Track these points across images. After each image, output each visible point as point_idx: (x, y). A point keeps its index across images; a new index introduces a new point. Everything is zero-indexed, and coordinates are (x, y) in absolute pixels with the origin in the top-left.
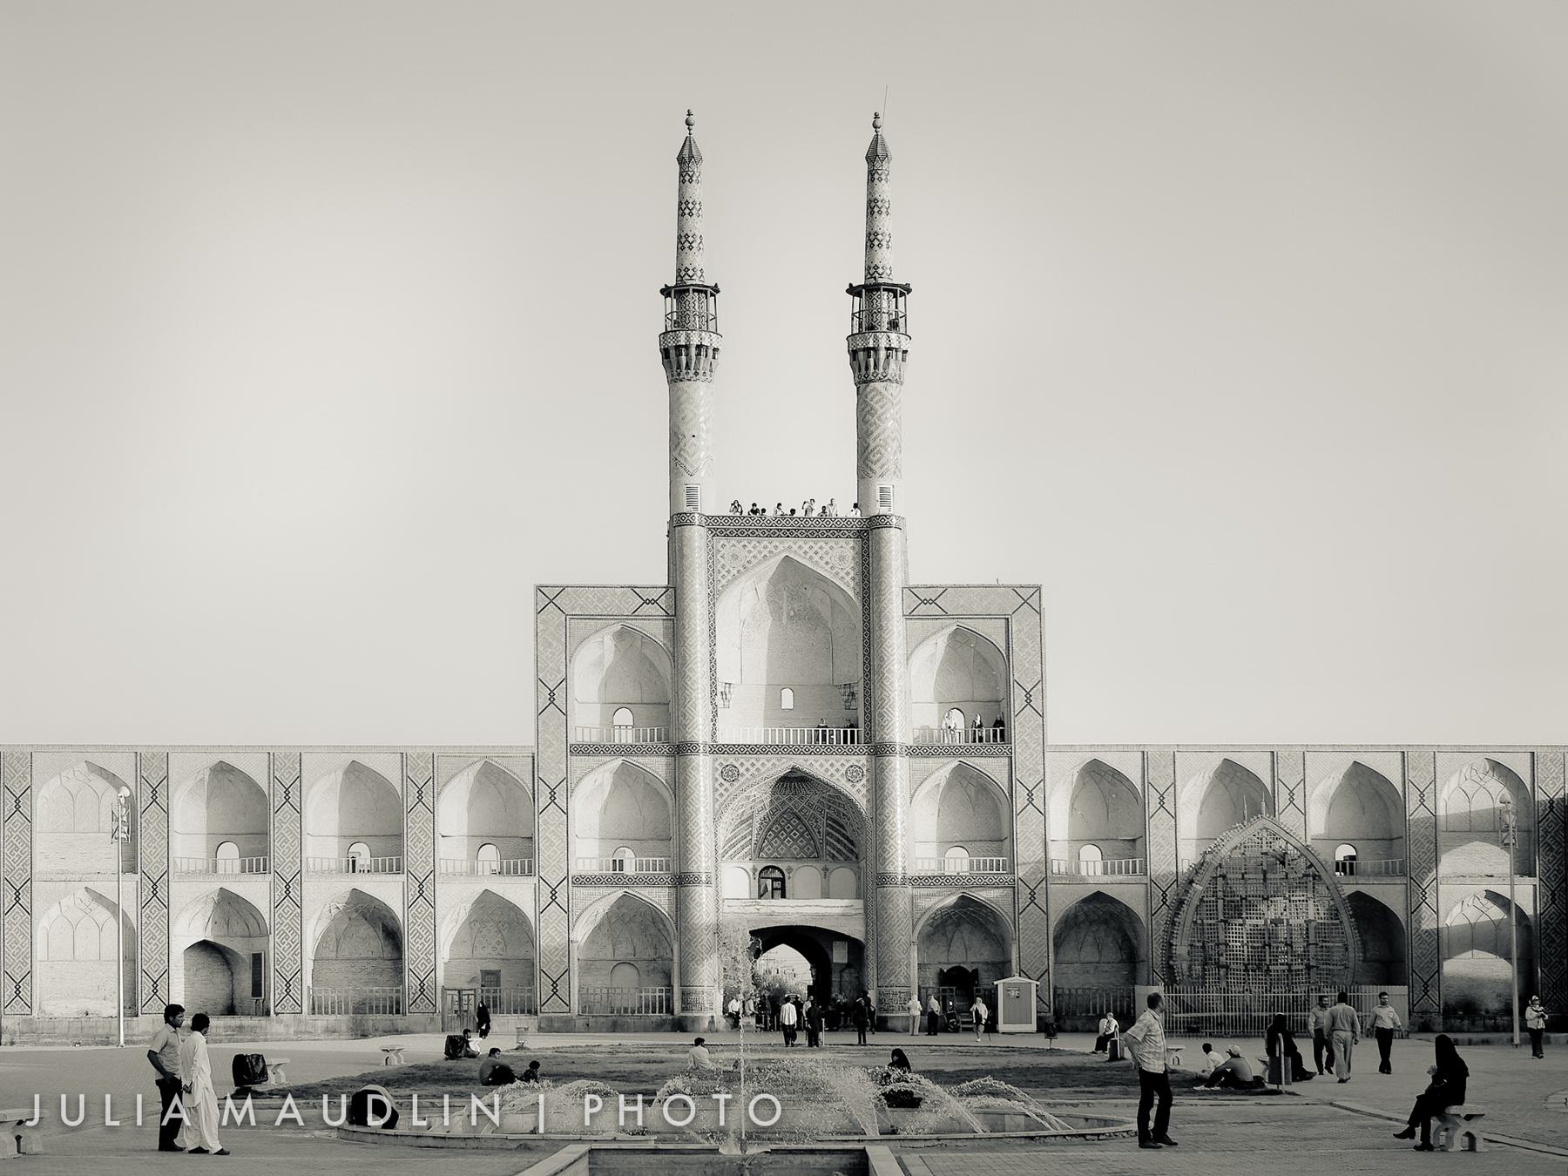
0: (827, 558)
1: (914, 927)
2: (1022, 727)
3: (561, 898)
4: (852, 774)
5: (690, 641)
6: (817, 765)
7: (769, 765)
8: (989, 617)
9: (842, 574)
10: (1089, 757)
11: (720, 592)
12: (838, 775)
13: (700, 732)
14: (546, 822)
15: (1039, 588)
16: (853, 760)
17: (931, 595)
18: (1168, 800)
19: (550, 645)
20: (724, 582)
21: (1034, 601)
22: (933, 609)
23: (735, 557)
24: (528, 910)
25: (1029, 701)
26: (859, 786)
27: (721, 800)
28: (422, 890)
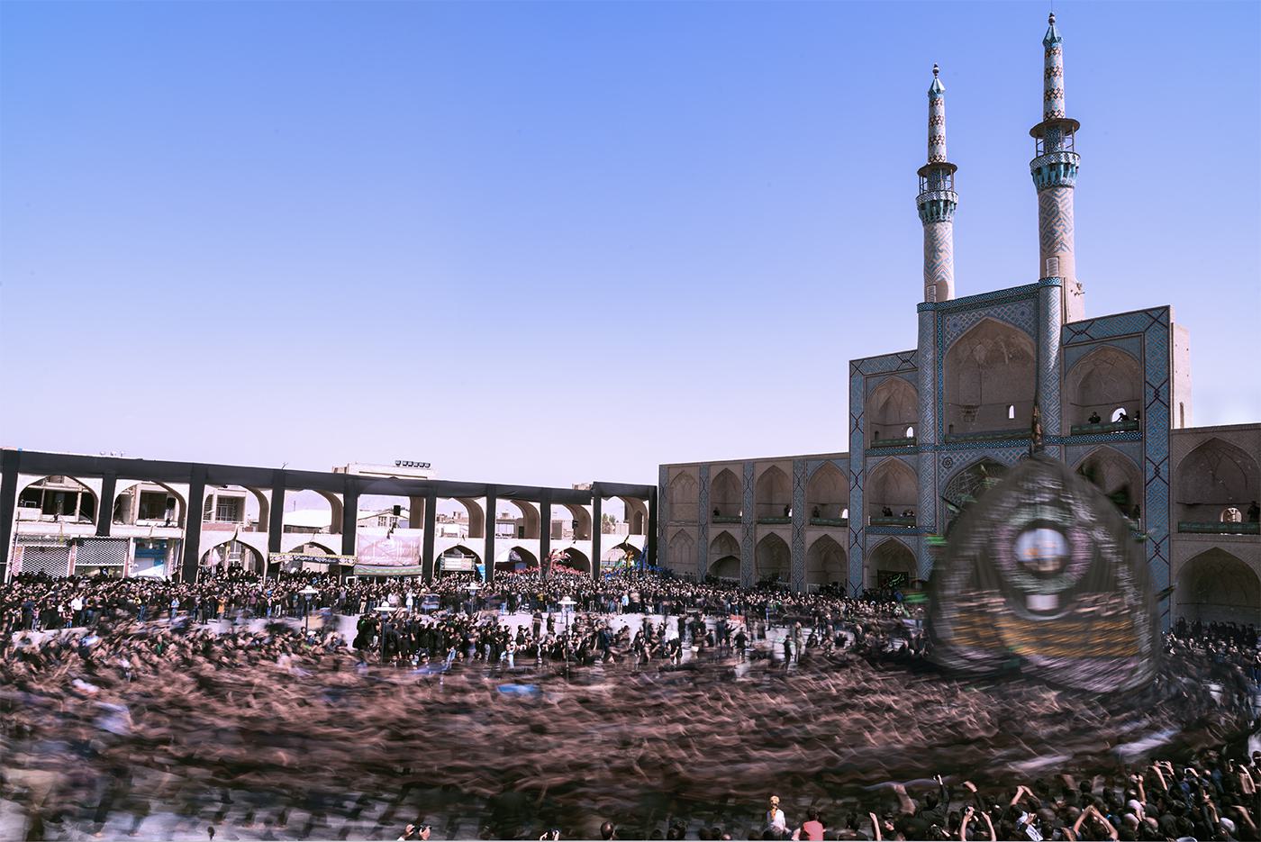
0: (1012, 315)
3: (860, 540)
8: (1128, 336)
14: (853, 496)
15: (1167, 308)
23: (955, 325)
28: (799, 534)
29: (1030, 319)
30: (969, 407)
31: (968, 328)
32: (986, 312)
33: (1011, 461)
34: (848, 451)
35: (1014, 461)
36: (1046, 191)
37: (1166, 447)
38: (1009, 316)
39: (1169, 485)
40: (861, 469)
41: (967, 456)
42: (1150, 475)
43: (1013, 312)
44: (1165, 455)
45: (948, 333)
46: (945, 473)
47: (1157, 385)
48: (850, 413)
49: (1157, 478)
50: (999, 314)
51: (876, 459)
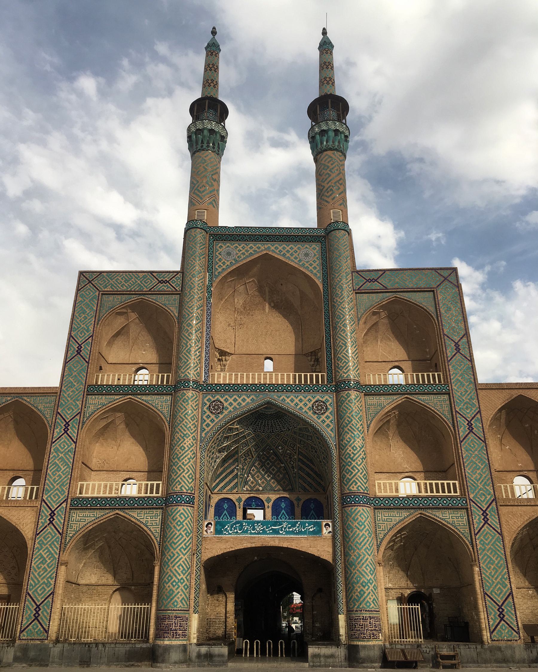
1: (378, 547)
2: (455, 369)
3: (58, 520)
4: (319, 408)
6: (288, 400)
7: (248, 400)
9: (307, 265)
10: (515, 393)
12: (305, 409)
14: (57, 451)
17: (374, 276)
20: (220, 270)
21: (452, 278)
23: (229, 254)
24: (27, 531)
26: (323, 417)
27: (207, 429)
29: (315, 262)
30: (223, 353)
31: (244, 258)
34: (56, 383)
35: (305, 409)
36: (329, 153)
37: (475, 401)
39: (485, 442)
40: (76, 411)
41: (244, 400)
42: (463, 431)
44: (475, 410)
45: (220, 260)
46: (212, 421)
47: (456, 339)
48: (70, 336)
49: (471, 434)
50: (280, 251)
51: (104, 399)
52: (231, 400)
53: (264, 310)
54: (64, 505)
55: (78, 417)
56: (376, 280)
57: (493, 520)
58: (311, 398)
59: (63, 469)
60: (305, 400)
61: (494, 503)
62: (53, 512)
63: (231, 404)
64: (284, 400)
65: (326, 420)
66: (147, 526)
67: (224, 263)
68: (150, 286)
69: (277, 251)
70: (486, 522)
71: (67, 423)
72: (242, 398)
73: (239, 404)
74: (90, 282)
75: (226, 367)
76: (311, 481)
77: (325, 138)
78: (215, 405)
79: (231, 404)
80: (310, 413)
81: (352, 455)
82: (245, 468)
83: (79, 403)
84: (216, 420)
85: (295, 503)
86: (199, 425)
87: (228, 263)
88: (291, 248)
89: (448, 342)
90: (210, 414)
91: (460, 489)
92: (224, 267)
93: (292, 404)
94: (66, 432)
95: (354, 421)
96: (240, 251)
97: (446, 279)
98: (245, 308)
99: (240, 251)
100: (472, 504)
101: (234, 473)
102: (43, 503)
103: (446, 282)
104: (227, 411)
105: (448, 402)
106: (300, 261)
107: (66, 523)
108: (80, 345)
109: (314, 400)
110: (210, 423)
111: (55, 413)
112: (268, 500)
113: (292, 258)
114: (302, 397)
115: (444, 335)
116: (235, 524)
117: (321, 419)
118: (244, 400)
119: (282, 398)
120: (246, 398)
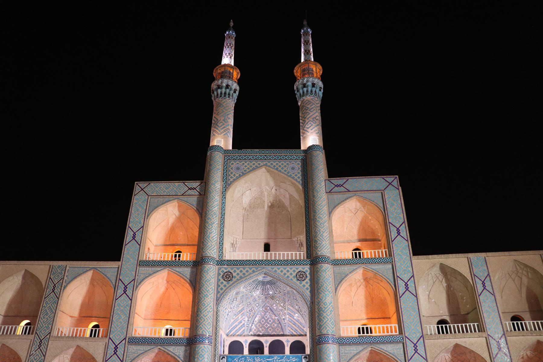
3: (120, 352)
5: (210, 204)
6: (279, 271)
7: (250, 271)
9: (293, 175)
11: (229, 185)
12: (291, 277)
13: (212, 251)
16: (300, 268)
18: (487, 284)
19: (138, 210)
20: (232, 180)
22: (342, 189)
23: (238, 169)
25: (399, 233)
26: (304, 283)
27: (221, 292)
29: (299, 173)
32: (264, 163)
33: (288, 277)
35: (291, 277)
37: (410, 269)
38: (282, 169)
39: (416, 296)
41: (247, 271)
43: (285, 166)
46: (225, 286)
50: (274, 166)
51: (150, 270)
52: (238, 271)
53: (264, 208)
54: (124, 342)
55: (133, 283)
56: (342, 186)
57: (421, 351)
58: (295, 270)
59: (123, 317)
60: (291, 271)
61: (422, 338)
62: (116, 346)
63: (238, 274)
64: (276, 271)
65: (305, 284)
66: (179, 358)
67: (234, 175)
68: (182, 192)
69: (272, 166)
70: (416, 352)
71: (126, 286)
72: (246, 270)
73: (244, 274)
74: (142, 189)
75: (237, 249)
76: (297, 329)
77: (305, 89)
78: (227, 275)
79: (238, 274)
80: (295, 280)
81: (324, 309)
82: (250, 319)
83: (134, 273)
84: (228, 286)
85: (285, 344)
86: (216, 289)
87: (238, 175)
88: (283, 164)
89: (392, 228)
90: (224, 281)
91: (399, 330)
92: (235, 178)
93: (282, 274)
94: (125, 292)
95: (325, 284)
96: (246, 166)
97: (390, 184)
98: (250, 207)
99: (246, 166)
100: (407, 339)
101: (242, 324)
102: (110, 340)
103: (390, 186)
104: (236, 279)
105: (391, 270)
106: (288, 173)
107: (125, 354)
108: (135, 233)
109: (297, 271)
110: (223, 287)
111: (118, 279)
112: (267, 341)
113: (283, 171)
114: (289, 269)
115: (390, 223)
116: (242, 357)
117: (302, 284)
118: (247, 271)
119: (274, 270)
120: (249, 270)
